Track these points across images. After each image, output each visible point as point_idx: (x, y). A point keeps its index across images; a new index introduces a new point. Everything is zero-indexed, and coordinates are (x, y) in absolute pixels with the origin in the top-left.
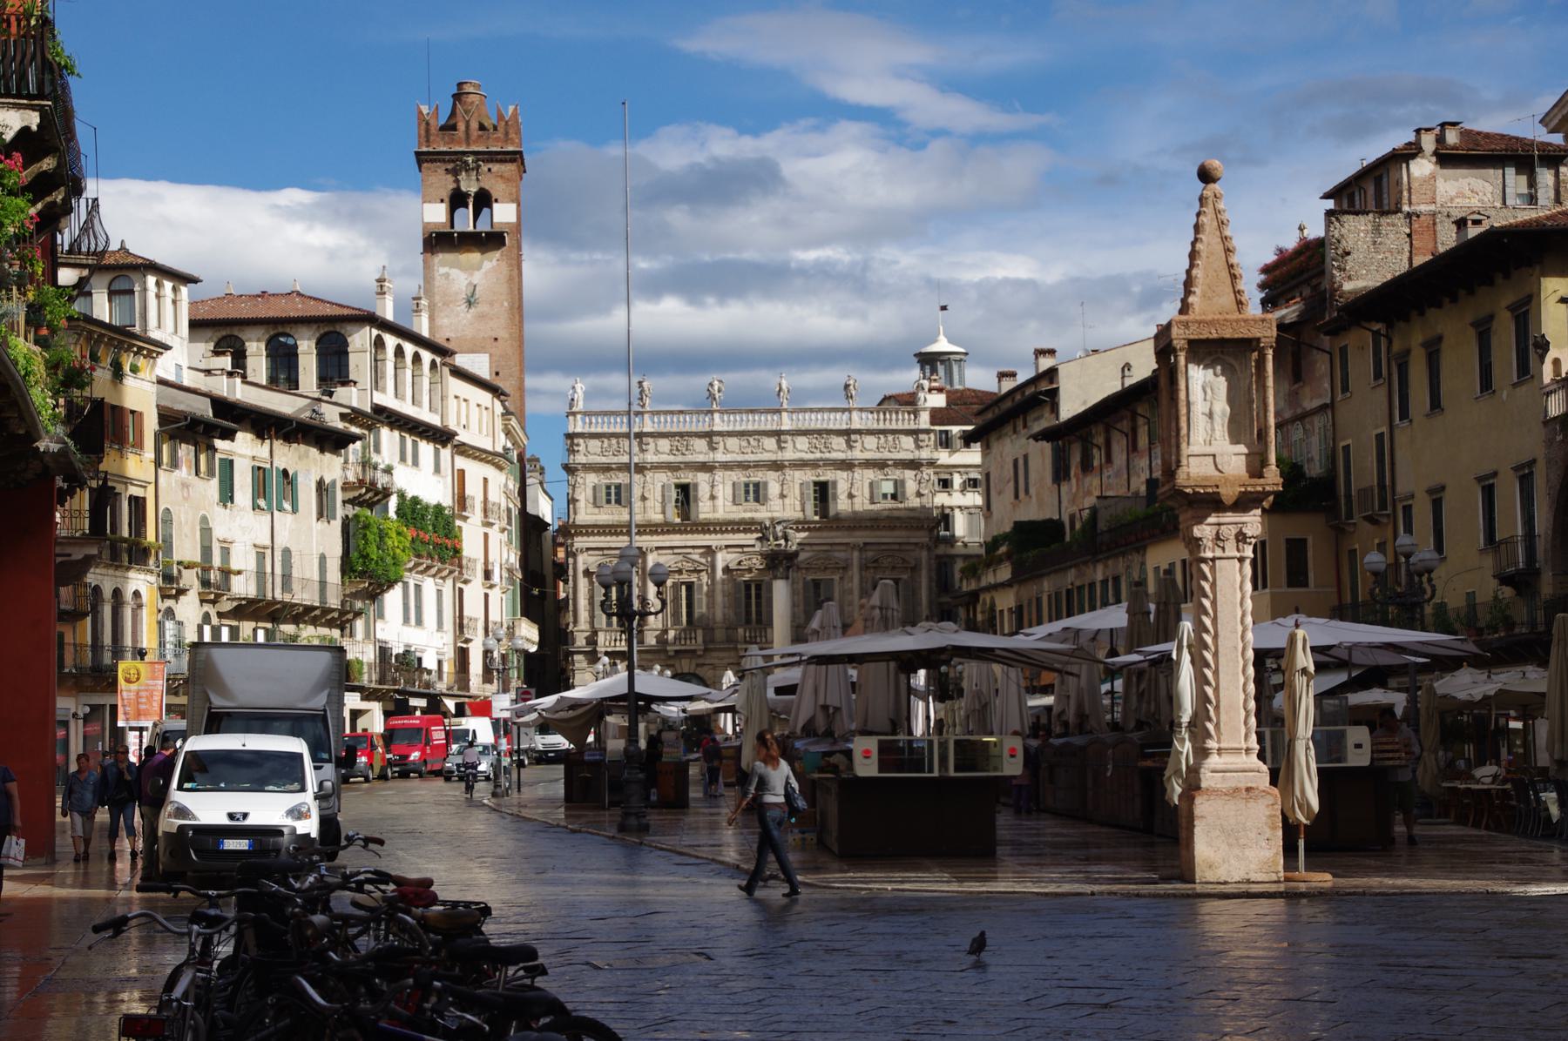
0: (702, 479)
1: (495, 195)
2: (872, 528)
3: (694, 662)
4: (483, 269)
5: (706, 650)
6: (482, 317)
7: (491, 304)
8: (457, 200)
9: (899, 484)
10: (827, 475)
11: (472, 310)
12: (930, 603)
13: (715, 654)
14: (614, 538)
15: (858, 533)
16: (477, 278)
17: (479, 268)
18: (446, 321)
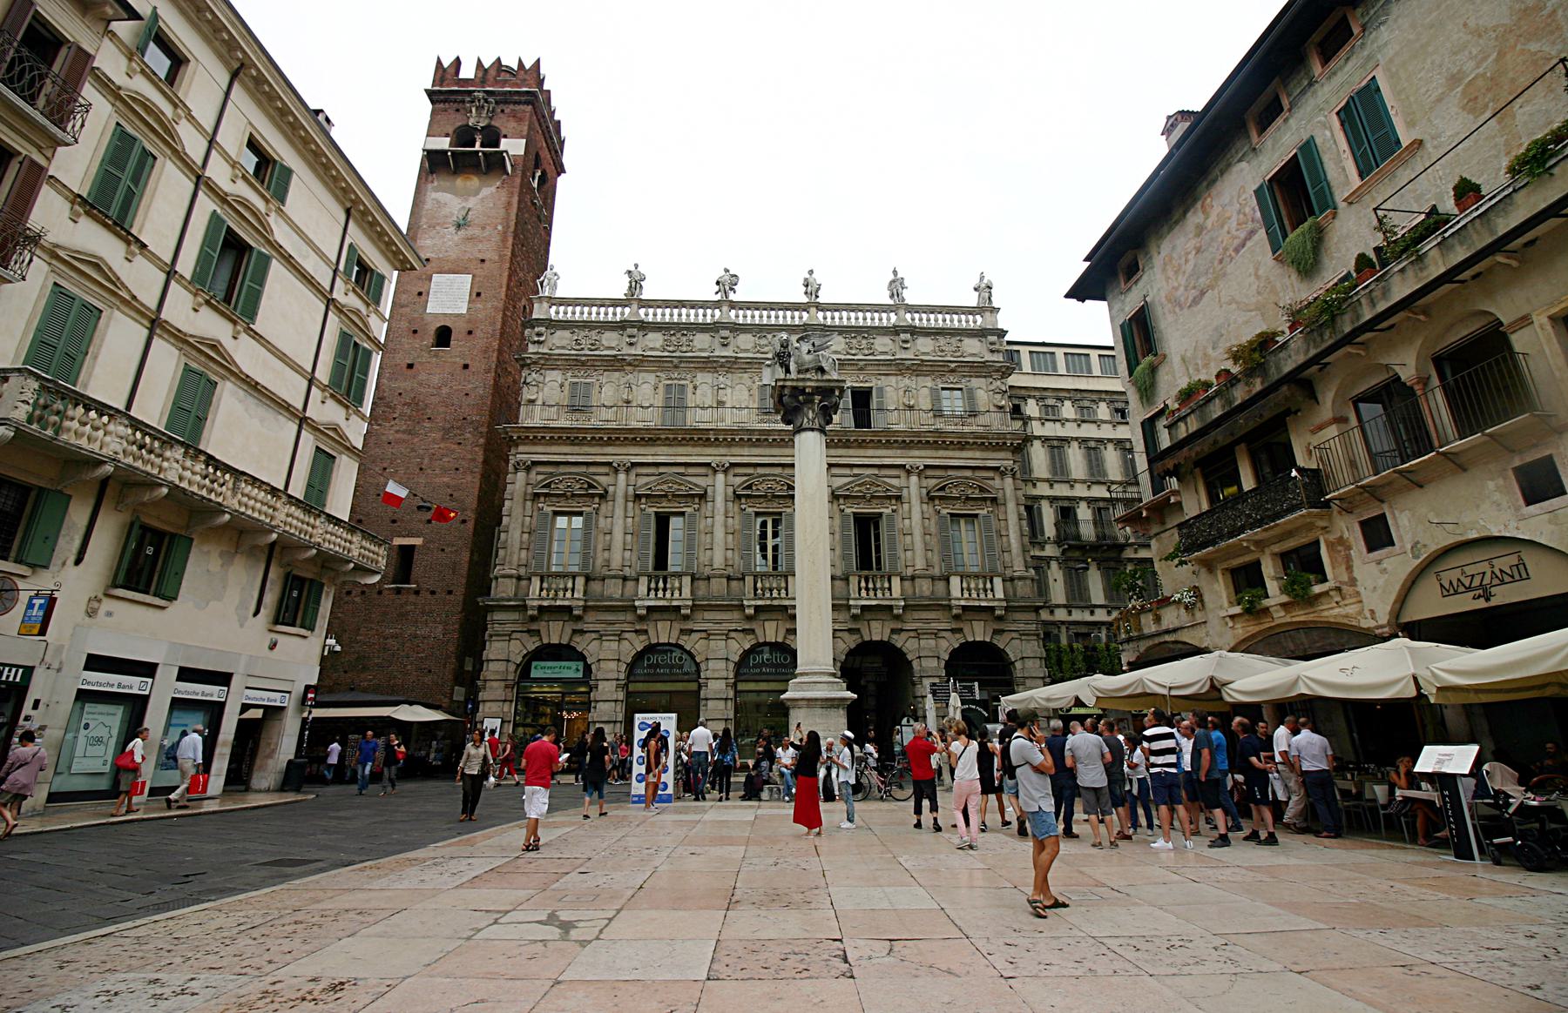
0: (704, 379)
1: (504, 132)
2: (934, 445)
3: (677, 626)
4: (482, 201)
5: (694, 608)
6: (470, 239)
7: (483, 228)
8: (464, 136)
9: (970, 396)
10: (872, 383)
11: (462, 233)
12: (1025, 551)
13: (708, 615)
14: (576, 449)
15: (917, 453)
16: (472, 202)
17: (477, 193)
18: (429, 242)
